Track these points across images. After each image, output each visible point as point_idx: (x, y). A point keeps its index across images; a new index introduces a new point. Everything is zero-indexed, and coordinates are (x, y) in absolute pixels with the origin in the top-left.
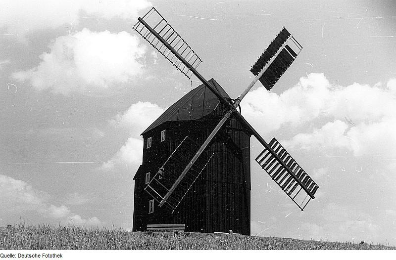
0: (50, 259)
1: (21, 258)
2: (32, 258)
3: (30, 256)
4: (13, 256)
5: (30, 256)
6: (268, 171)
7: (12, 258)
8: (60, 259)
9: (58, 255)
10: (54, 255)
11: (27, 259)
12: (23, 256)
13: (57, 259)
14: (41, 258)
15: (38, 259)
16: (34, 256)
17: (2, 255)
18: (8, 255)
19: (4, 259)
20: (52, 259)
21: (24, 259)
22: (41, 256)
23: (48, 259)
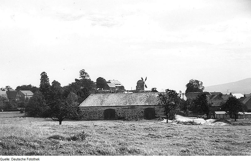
0: (32, 161)
1: (14, 161)
2: (20, 161)
3: (19, 160)
4: (8, 159)
5: (19, 160)
7: (8, 161)
8: (38, 161)
9: (37, 159)
10: (34, 159)
11: (17, 161)
12: (14, 159)
13: (36, 161)
14: (26, 161)
15: (24, 161)
16: (21, 159)
17: (1, 159)
18: (5, 159)
19: (3, 161)
20: (33, 161)
21: (15, 161)
23: (30, 161)
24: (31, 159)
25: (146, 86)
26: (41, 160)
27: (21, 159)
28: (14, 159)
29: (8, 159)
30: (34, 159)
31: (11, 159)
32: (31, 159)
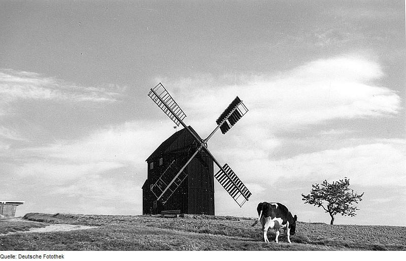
3: (31, 257)
4: (13, 257)
5: (31, 257)
6: (233, 196)
9: (60, 256)
10: (55, 256)
12: (23, 257)
16: (34, 257)
18: (9, 256)
27: (34, 257)
28: (23, 257)
29: (13, 257)
30: (55, 256)
31: (17, 257)
32: (50, 257)
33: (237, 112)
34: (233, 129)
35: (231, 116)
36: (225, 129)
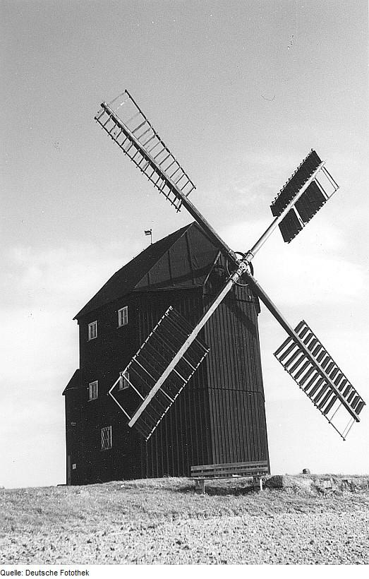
3: (43, 573)
4: (18, 573)
5: (43, 573)
8: (85, 577)
9: (83, 572)
12: (32, 573)
13: (82, 577)
16: (48, 573)
17: (3, 573)
18: (12, 572)
22: (59, 573)
24: (69, 573)
25: (305, 350)
26: (91, 575)
27: (48, 573)
28: (32, 573)
29: (18, 573)
31: (24, 573)
32: (69, 573)
33: (314, 187)
34: (311, 230)
35: (298, 203)
36: (290, 230)
